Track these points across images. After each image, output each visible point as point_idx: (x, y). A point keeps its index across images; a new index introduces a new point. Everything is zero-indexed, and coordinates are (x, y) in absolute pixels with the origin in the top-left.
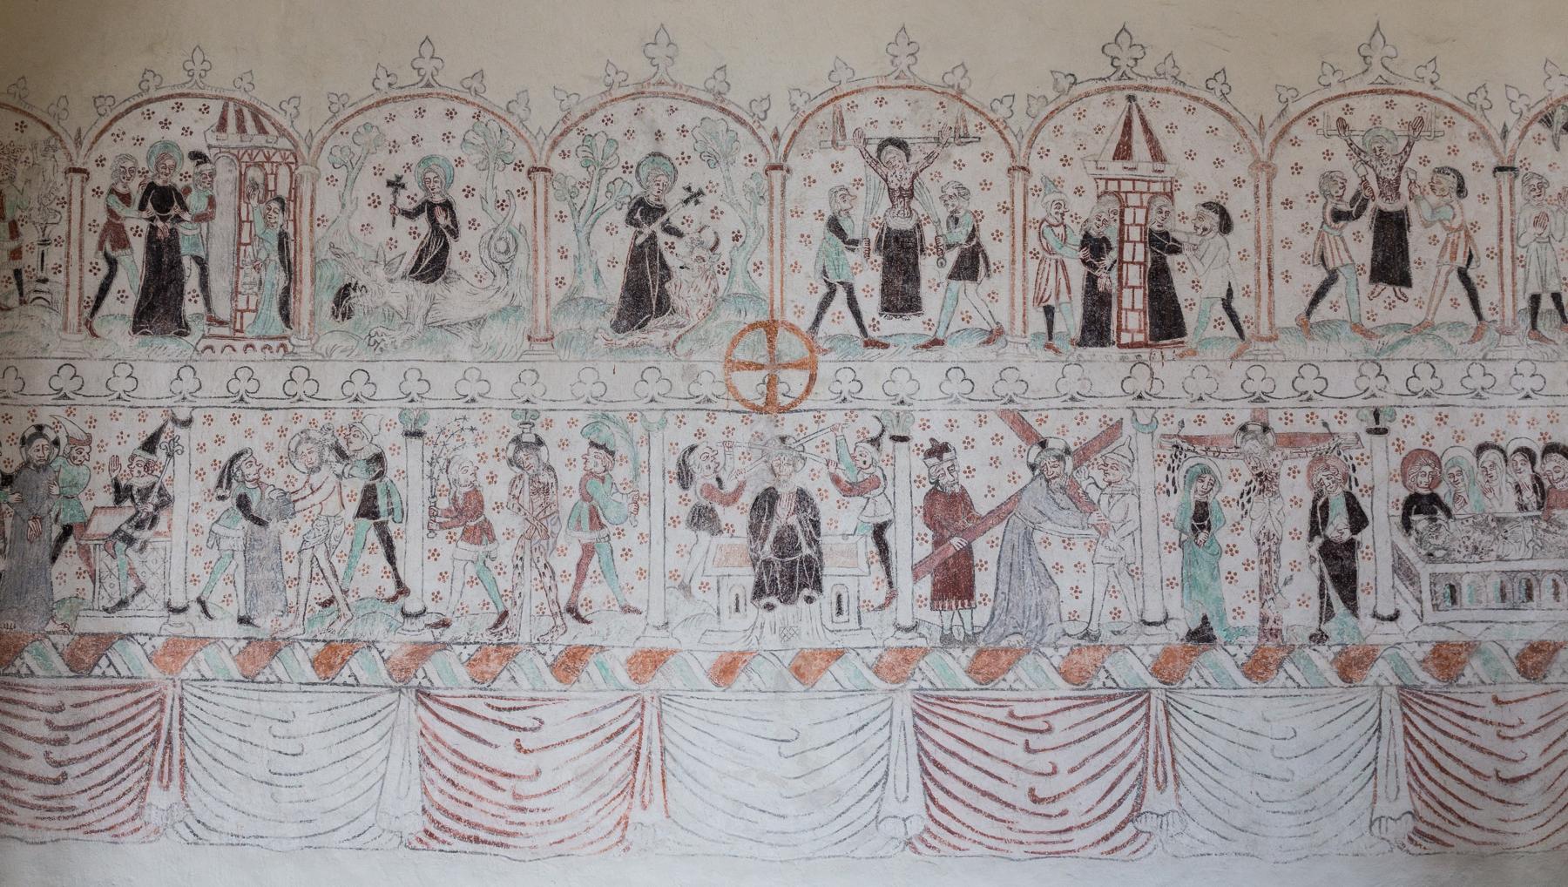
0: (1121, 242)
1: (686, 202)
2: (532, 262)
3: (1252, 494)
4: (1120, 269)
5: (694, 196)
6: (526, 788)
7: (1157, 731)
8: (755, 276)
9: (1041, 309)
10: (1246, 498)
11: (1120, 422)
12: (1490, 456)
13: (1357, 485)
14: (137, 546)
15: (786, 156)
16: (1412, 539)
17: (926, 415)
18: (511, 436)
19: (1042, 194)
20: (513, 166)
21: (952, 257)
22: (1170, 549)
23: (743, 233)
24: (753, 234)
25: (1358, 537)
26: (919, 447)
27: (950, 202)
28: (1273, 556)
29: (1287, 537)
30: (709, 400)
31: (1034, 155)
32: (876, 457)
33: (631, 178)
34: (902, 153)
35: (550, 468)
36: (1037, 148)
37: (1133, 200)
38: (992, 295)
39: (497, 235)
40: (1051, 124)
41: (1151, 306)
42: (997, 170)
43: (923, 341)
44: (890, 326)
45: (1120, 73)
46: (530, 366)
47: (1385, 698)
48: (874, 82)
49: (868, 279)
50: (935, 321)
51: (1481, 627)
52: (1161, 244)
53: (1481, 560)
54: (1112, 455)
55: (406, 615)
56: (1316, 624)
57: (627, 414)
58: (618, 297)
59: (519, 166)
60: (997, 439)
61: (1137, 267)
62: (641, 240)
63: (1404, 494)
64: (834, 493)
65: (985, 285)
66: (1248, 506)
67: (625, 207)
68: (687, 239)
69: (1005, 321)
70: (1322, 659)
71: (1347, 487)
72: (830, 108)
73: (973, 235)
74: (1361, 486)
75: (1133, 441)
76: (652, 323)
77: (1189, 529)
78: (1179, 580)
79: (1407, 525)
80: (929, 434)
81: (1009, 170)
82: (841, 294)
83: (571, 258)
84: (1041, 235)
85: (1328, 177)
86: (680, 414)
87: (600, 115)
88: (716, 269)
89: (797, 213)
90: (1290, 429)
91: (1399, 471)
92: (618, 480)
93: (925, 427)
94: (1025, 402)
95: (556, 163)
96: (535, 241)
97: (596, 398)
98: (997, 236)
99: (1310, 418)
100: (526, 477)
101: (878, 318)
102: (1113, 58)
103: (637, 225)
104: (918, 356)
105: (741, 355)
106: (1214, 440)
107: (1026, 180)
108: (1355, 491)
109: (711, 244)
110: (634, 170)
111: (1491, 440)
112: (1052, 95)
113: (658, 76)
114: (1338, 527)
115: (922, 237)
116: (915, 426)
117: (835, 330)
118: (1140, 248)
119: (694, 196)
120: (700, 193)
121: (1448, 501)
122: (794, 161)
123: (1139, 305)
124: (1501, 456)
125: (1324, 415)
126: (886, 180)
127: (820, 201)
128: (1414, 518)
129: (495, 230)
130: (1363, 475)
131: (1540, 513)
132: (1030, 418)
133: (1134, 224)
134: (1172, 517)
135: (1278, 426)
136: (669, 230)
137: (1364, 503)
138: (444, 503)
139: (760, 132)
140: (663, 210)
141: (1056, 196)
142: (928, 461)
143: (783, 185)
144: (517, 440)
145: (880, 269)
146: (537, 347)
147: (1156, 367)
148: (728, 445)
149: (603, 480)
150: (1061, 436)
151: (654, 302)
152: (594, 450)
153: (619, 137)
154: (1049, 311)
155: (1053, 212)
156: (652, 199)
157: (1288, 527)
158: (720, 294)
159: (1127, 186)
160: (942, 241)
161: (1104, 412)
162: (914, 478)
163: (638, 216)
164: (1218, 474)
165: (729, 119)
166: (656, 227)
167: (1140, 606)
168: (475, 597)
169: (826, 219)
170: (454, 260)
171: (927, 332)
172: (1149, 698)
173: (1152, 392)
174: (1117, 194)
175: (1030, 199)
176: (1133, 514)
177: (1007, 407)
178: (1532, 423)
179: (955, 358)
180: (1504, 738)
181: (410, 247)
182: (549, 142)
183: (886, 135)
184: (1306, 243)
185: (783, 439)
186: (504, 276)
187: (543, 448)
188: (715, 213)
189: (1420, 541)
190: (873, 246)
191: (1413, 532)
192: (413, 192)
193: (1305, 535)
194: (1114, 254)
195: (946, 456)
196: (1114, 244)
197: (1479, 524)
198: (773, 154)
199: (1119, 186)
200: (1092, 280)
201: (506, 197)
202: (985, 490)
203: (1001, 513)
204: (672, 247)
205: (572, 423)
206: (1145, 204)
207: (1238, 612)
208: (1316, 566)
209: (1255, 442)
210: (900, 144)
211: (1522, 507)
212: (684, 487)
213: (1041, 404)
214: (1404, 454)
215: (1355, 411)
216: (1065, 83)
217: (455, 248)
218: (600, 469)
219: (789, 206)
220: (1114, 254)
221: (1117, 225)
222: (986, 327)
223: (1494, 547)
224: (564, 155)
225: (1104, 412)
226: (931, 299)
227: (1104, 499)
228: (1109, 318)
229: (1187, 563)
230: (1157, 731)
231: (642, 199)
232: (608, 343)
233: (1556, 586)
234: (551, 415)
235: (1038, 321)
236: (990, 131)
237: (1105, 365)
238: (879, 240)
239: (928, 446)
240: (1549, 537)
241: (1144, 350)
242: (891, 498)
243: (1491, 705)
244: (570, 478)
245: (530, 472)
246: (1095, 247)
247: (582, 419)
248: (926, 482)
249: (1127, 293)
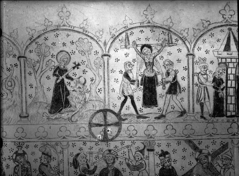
0: (227, 80)
1: (74, 68)
2: (20, 89)
4: (227, 90)
5: (77, 66)
8: (99, 93)
9: (199, 104)
11: (227, 144)
15: (109, 52)
17: (160, 142)
18: (14, 151)
19: (199, 63)
20: (12, 56)
21: (168, 86)
23: (94, 78)
24: (98, 79)
26: (157, 153)
27: (166, 67)
30: (84, 138)
31: (196, 50)
32: (142, 157)
33: (54, 60)
34: (149, 50)
35: (28, 162)
36: (197, 47)
37: (231, 65)
38: (182, 99)
39: (8, 80)
40: (202, 38)
41: (237, 102)
42: (183, 55)
43: (157, 115)
44: (146, 110)
45: (225, 20)
46: (20, 126)
48: (139, 25)
49: (138, 95)
50: (162, 109)
54: (224, 155)
57: (55, 143)
58: (51, 102)
59: (15, 56)
61: (232, 89)
62: (59, 81)
64: (128, 170)
65: (180, 96)
67: (53, 70)
68: (75, 81)
69: (186, 108)
72: (124, 34)
73: (175, 78)
75: (232, 150)
76: (63, 110)
80: (161, 148)
81: (187, 55)
82: (129, 100)
83: (34, 88)
84: (198, 78)
86: (74, 142)
87: (43, 37)
88: (85, 91)
89: (113, 71)
92: (52, 166)
93: (159, 146)
94: (194, 137)
95: (28, 55)
96: (21, 82)
97: (44, 137)
98: (183, 79)
100: (20, 165)
101: (142, 108)
102: (223, 15)
103: (57, 76)
104: (156, 121)
105: (95, 121)
107: (193, 59)
109: (83, 81)
110: (55, 57)
112: (202, 28)
113: (63, 23)
115: (157, 80)
116: (156, 146)
117: (127, 112)
118: (234, 82)
119: (77, 66)
120: (79, 65)
122: (112, 53)
123: (233, 102)
126: (144, 59)
127: (121, 67)
129: (7, 78)
132: (196, 142)
133: (231, 74)
136: (68, 77)
139: (100, 43)
140: (66, 71)
141: (204, 64)
142: (160, 158)
143: (108, 61)
144: (16, 153)
145: (142, 90)
146: (23, 119)
148: (91, 153)
149: (47, 166)
150: (207, 149)
151: (64, 103)
152: (43, 156)
153: (50, 45)
154: (202, 105)
155: (203, 70)
156: (62, 67)
158: (87, 100)
159: (228, 60)
160: (164, 80)
161: (221, 140)
162: (156, 164)
163: (57, 73)
165: (89, 38)
166: (64, 77)
169: (123, 73)
171: (159, 112)
174: (225, 63)
175: (195, 66)
177: (188, 138)
179: (169, 122)
182: (25, 47)
183: (144, 43)
185: (110, 151)
186: (11, 94)
187: (26, 155)
188: (84, 72)
190: (140, 83)
194: (224, 84)
195: (167, 156)
196: (224, 81)
198: (104, 50)
199: (226, 60)
200: (216, 94)
201: (10, 67)
202: (181, 168)
204: (70, 84)
205: (36, 146)
206: (235, 67)
210: (149, 47)
212: (76, 168)
213: (200, 137)
216: (206, 24)
218: (45, 162)
219: (110, 69)
220: (224, 84)
221: (225, 74)
222: (180, 111)
224: (31, 52)
225: (221, 140)
226: (160, 102)
227: (222, 170)
228: (223, 106)
231: (58, 67)
232: (48, 118)
234: (28, 143)
235: (198, 108)
236: (180, 42)
238: (142, 80)
239: (160, 153)
241: (236, 118)
242: (148, 171)
245: (21, 164)
247: (39, 144)
248: (160, 165)
249: (229, 98)
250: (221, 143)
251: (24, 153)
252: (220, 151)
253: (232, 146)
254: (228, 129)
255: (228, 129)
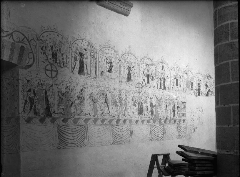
6: (122, 136)
14: (81, 105)
44: (147, 85)
52: (164, 79)
55: (110, 115)
60: (154, 98)
85: (174, 75)
95: (122, 60)
136: (131, 70)
138: (113, 101)
166: (130, 70)
168: (116, 113)
170: (112, 71)
181: (108, 67)
184: (172, 81)
192: (108, 61)
200: (160, 82)
203: (155, 106)
217: (112, 68)
226: (150, 82)
237: (161, 91)
244: (124, 99)
246: (160, 79)
251: (121, 95)
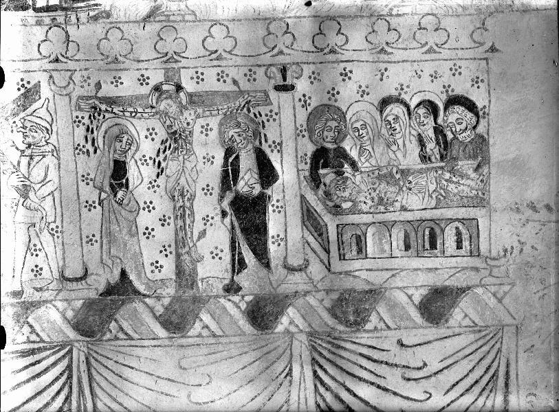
3: (168, 152)
7: (80, 382)
10: (162, 156)
12: (396, 109)
13: (266, 141)
16: (321, 192)
22: (90, 207)
25: (268, 192)
28: (188, 212)
29: (199, 193)
47: (296, 343)
51: (388, 274)
53: (387, 211)
54: (29, 118)
56: (228, 276)
63: (310, 149)
66: (163, 165)
70: (234, 308)
71: (257, 143)
74: (270, 142)
77: (108, 189)
78: (98, 237)
79: (315, 180)
90: (202, 88)
91: (305, 126)
99: (220, 77)
106: (131, 101)
108: (265, 147)
111: (394, 93)
114: (248, 182)
121: (354, 154)
124: (405, 110)
125: (233, 73)
128: (322, 171)
130: (271, 132)
131: (443, 164)
134: (92, 176)
135: (189, 86)
137: (274, 159)
147: (72, 30)
157: (201, 184)
164: (136, 135)
167: (61, 264)
172: (70, 351)
173: (69, 54)
176: (53, 174)
178: (434, 77)
180: (409, 380)
189: (327, 194)
191: (322, 186)
193: (216, 191)
197: (385, 176)
207: (157, 266)
208: (227, 220)
209: (169, 101)
211: (424, 158)
214: (310, 109)
215: (263, 69)
223: (399, 198)
229: (105, 221)
230: (80, 382)
233: (459, 234)
240: (452, 187)
241: (59, 13)
243: (395, 349)
250: (21, 83)
252: (19, 106)
253: (52, 93)
254: (39, 45)
255: (39, 45)
